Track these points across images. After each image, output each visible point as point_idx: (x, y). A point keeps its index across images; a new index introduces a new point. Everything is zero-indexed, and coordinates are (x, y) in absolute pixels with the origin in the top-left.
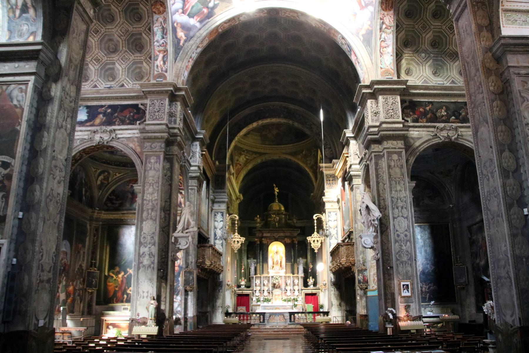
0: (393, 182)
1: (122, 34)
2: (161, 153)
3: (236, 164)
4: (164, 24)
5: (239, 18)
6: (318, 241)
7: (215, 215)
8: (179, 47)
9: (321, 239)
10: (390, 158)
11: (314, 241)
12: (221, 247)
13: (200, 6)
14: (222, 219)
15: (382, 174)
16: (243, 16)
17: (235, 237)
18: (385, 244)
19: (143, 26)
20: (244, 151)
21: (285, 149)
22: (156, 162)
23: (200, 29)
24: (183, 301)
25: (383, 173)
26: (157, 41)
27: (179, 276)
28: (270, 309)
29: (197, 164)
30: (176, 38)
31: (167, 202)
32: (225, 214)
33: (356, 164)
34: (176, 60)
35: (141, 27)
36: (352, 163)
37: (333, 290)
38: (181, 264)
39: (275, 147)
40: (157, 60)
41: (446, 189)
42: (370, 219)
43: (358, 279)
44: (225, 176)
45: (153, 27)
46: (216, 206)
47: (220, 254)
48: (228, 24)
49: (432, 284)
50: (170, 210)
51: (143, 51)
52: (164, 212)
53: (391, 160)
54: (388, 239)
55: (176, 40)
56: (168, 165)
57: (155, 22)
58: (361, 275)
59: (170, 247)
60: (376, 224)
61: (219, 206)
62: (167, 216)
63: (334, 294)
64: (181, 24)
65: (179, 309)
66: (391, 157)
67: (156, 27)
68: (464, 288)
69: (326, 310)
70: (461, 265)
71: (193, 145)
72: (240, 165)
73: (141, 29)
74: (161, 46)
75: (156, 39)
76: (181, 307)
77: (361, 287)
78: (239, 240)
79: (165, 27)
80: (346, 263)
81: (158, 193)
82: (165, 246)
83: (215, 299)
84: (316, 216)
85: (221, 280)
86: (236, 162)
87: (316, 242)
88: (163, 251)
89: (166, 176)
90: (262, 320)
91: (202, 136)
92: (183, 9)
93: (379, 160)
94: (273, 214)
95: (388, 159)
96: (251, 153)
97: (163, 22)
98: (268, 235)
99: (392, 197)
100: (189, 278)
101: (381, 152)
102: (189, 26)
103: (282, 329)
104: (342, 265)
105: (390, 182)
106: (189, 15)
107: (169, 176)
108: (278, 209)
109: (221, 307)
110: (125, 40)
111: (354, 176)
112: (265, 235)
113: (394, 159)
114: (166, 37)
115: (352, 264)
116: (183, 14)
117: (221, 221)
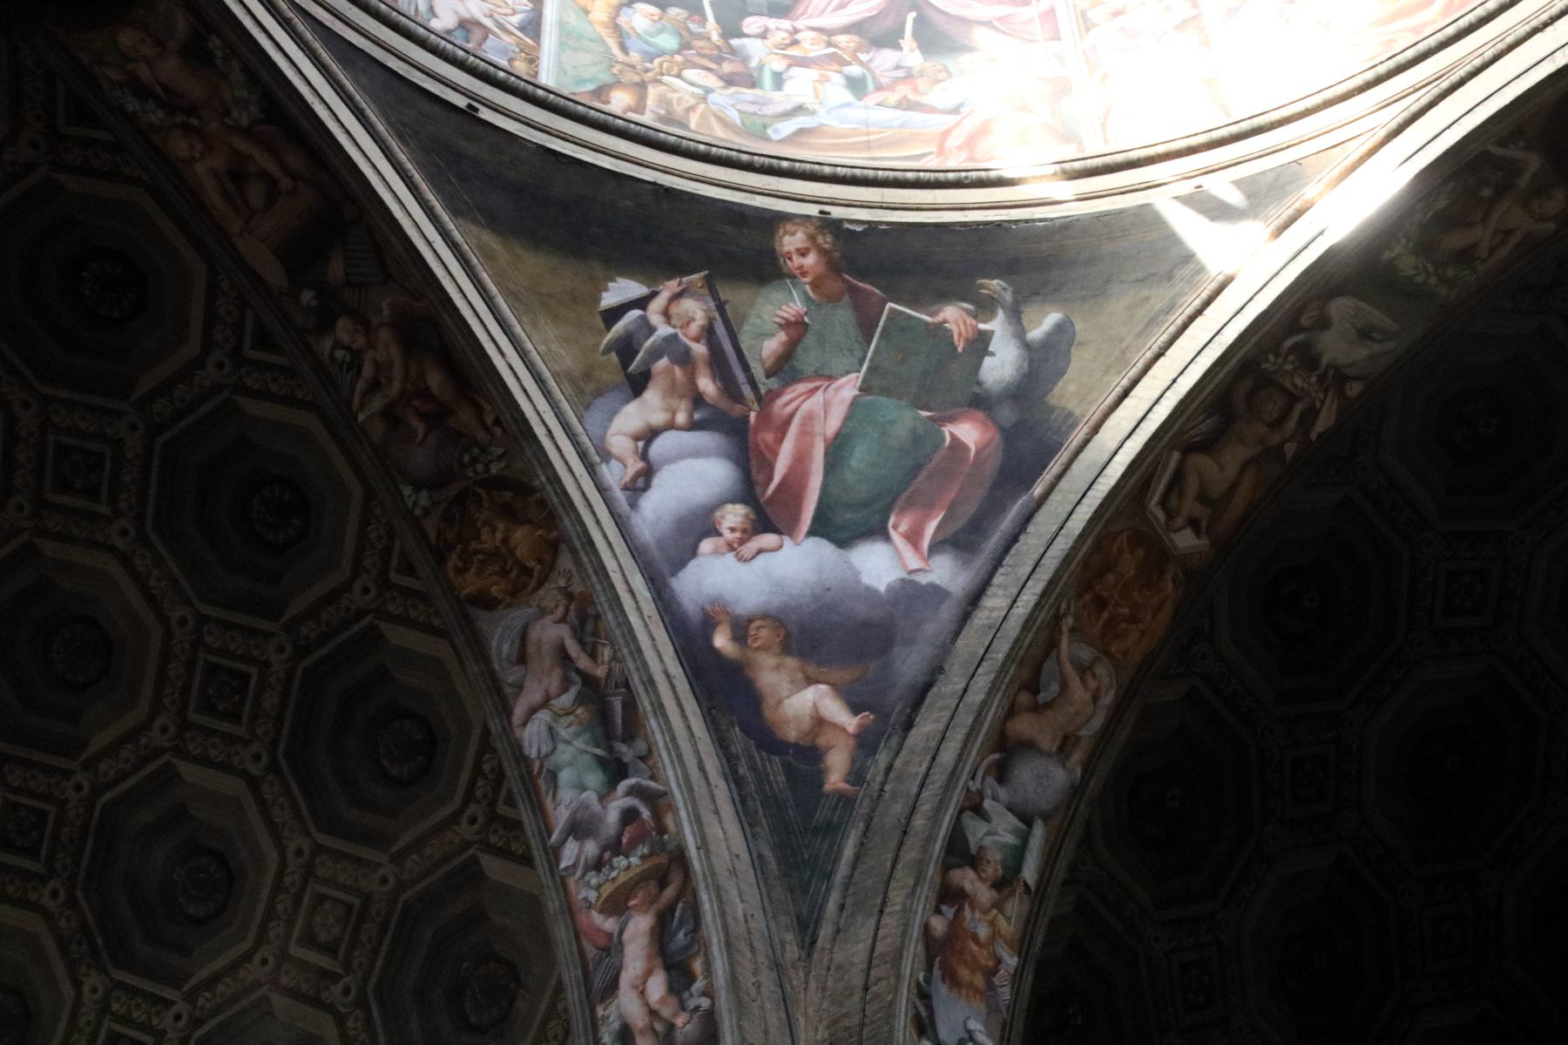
1: (325, 962)
4: (593, 655)
5: (1308, 358)
8: (819, 816)
13: (903, 419)
16: (1339, 308)
19: (469, 798)
23: (975, 598)
26: (579, 828)
30: (766, 738)
34: (807, 928)
35: (455, 818)
40: (612, 987)
45: (507, 731)
48: (1233, 456)
51: (521, 1005)
55: (775, 768)
57: (511, 676)
64: (775, 618)
67: (533, 711)
73: (465, 831)
74: (615, 847)
75: (560, 817)
79: (601, 672)
92: (748, 491)
97: (573, 649)
102: (861, 610)
106: (824, 527)
110: (362, 1002)
114: (641, 746)
116: (769, 539)
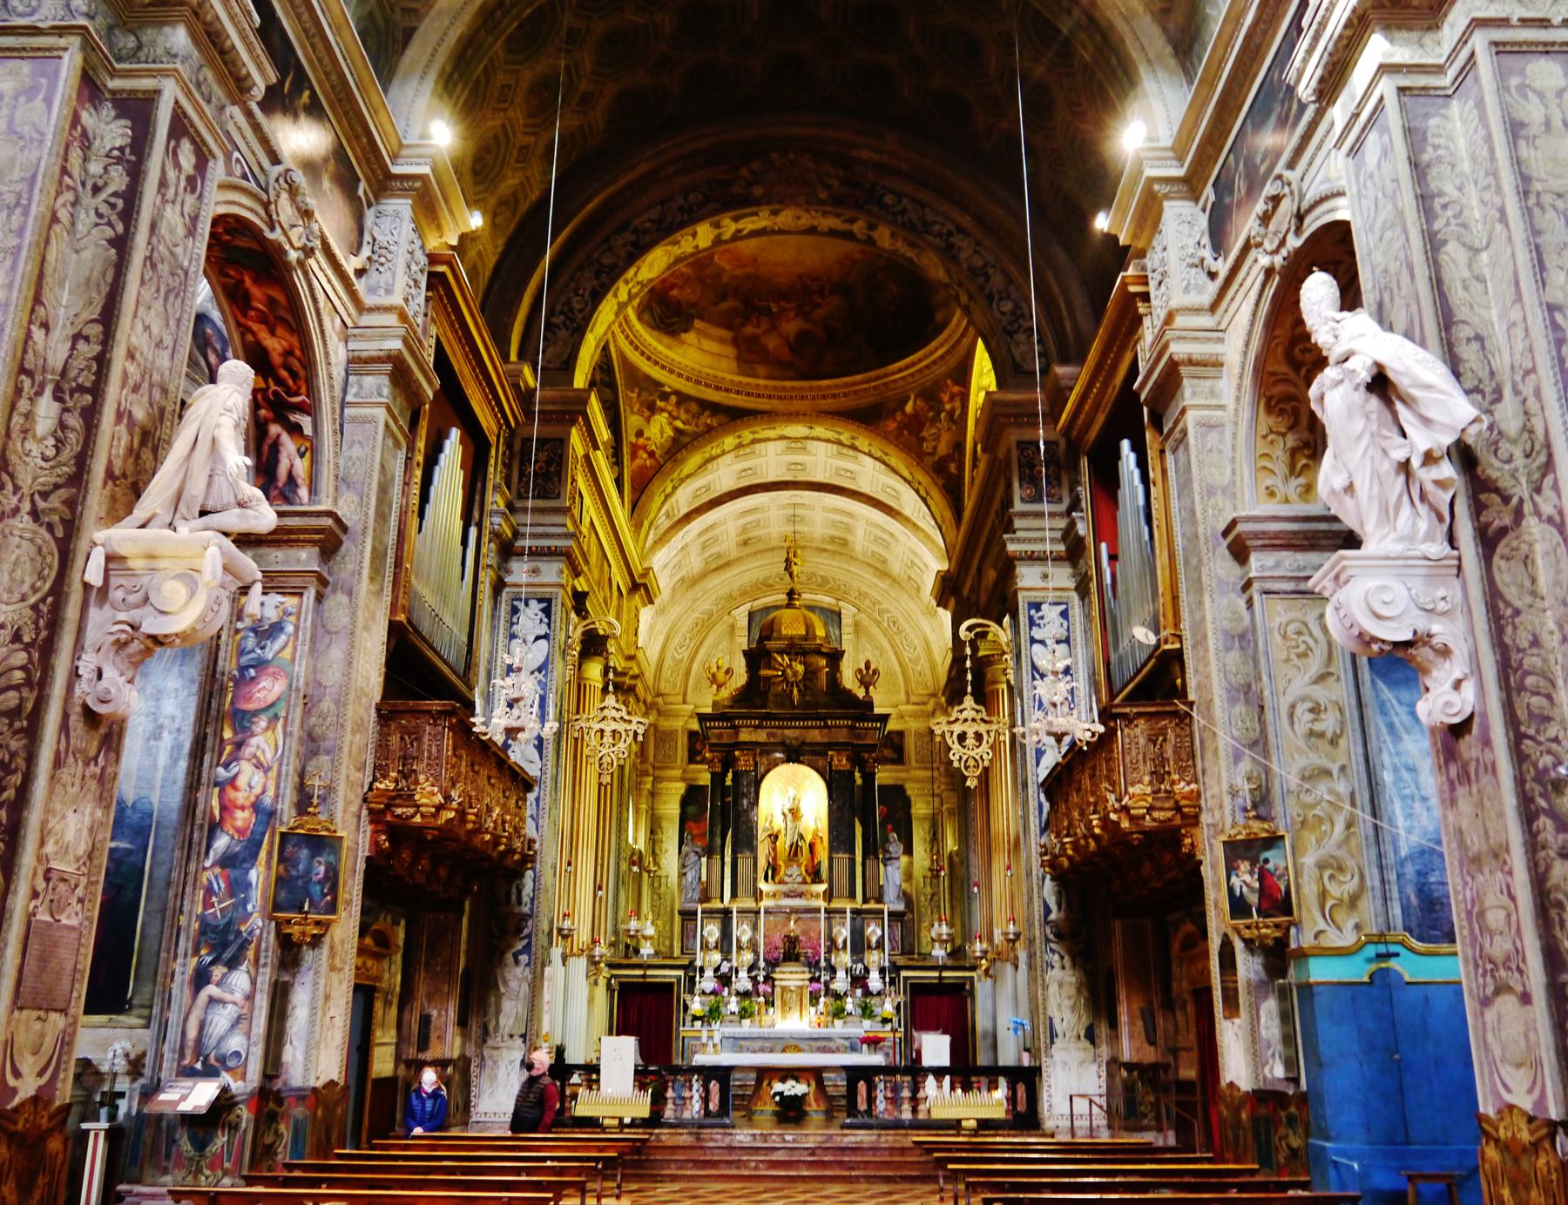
0: (1551, 214)
2: (62, 42)
3: (635, 449)
6: (979, 737)
7: (515, 611)
9: (994, 727)
10: (1514, 82)
11: (962, 737)
12: (535, 755)
14: (543, 630)
15: (1455, 194)
17: (606, 712)
18: (1517, 612)
20: (665, 397)
21: (834, 396)
22: (31, 92)
24: (262, 1002)
25: (1460, 189)
27: (255, 856)
28: (762, 1050)
29: (397, 299)
31: (87, 339)
32: (557, 610)
33: (1196, 310)
36: (1174, 304)
37: (1057, 965)
38: (271, 792)
39: (793, 388)
42: (1399, 455)
43: (1231, 890)
44: (562, 442)
46: (520, 572)
47: (522, 783)
50: (97, 390)
52: (58, 396)
53: (1523, 89)
54: (1534, 580)
56: (112, 132)
58: (1244, 866)
59: (72, 612)
60: (1441, 484)
61: (535, 571)
62: (74, 421)
63: (1061, 985)
65: (235, 1043)
66: (1522, 72)
69: (1009, 1055)
71: (379, 215)
72: (652, 454)
76: (248, 1035)
77: (1247, 934)
78: (621, 727)
80: (1150, 809)
81: (13, 268)
82: (35, 607)
83: (493, 999)
84: (970, 629)
85: (526, 909)
86: (633, 440)
87: (970, 741)
88: (17, 637)
89: (96, 190)
90: (713, 1106)
91: (425, 170)
93: (1427, 116)
94: (781, 652)
95: (1502, 87)
96: (694, 407)
98: (761, 736)
99: (1551, 308)
100: (308, 871)
101: (1439, 69)
103: (812, 1151)
104: (1132, 819)
105: (1528, 213)
107: (115, 194)
108: (802, 632)
109: (523, 1036)
111: (1191, 362)
112: (745, 736)
113: (1538, 85)
115: (1184, 816)
117: (538, 638)
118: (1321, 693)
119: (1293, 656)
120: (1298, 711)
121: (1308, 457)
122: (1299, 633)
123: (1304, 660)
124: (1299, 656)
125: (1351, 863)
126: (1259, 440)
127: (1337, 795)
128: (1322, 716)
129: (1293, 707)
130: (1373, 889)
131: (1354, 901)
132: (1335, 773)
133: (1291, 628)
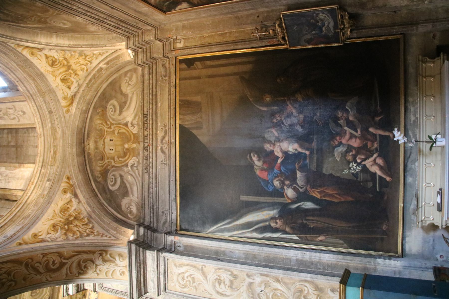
41: (101, 69)
49: (340, 114)
68: (353, 17)
70: (281, 26)
118: (212, 276)
119: (194, 285)
120: (220, 291)
121: (106, 254)
122: (183, 278)
123: (196, 280)
124: (194, 282)
125: (298, 285)
126: (99, 277)
127: (262, 282)
128: (222, 279)
129: (218, 292)
130: (311, 278)
131: (317, 288)
132: (252, 281)
133: (181, 281)
